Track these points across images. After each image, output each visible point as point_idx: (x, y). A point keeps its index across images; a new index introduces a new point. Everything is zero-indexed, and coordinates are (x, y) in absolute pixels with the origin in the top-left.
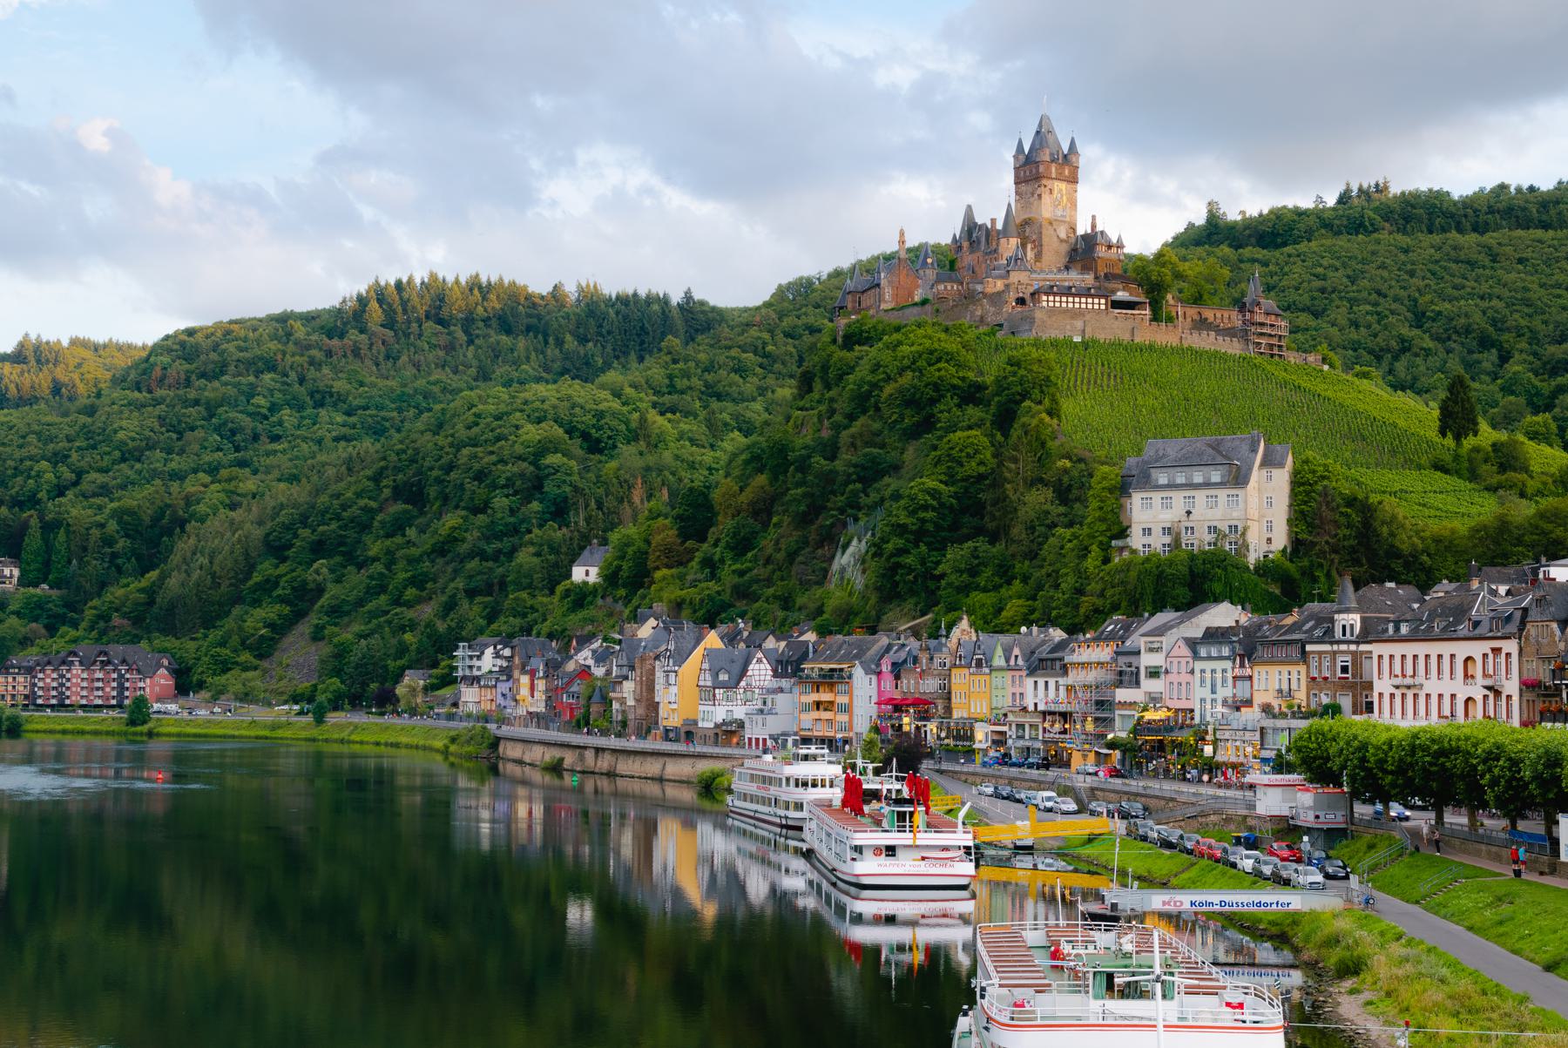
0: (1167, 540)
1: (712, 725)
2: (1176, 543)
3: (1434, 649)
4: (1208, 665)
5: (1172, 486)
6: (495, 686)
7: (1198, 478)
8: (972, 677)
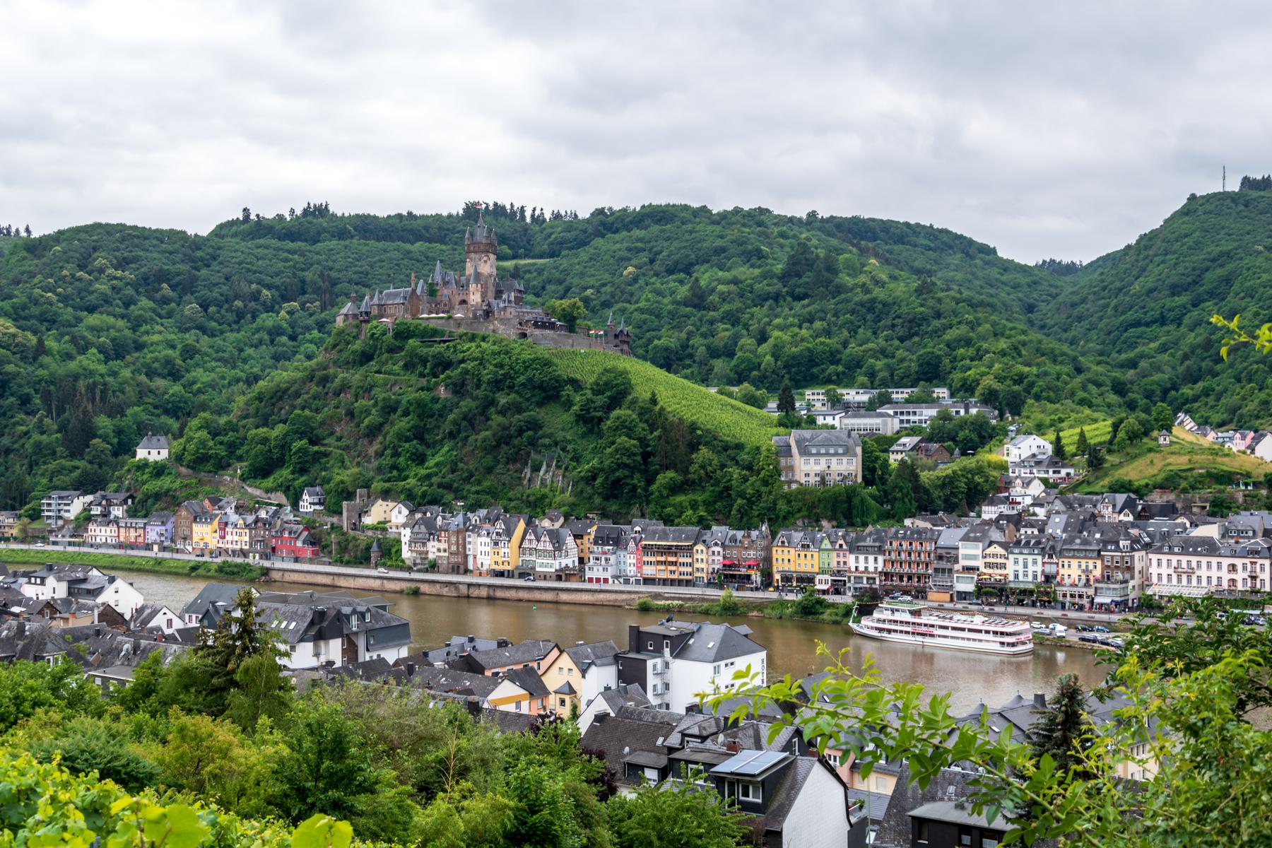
0: (818, 479)
2: (823, 482)
3: (1204, 560)
4: (1021, 558)
5: (818, 454)
6: (144, 528)
7: (823, 451)
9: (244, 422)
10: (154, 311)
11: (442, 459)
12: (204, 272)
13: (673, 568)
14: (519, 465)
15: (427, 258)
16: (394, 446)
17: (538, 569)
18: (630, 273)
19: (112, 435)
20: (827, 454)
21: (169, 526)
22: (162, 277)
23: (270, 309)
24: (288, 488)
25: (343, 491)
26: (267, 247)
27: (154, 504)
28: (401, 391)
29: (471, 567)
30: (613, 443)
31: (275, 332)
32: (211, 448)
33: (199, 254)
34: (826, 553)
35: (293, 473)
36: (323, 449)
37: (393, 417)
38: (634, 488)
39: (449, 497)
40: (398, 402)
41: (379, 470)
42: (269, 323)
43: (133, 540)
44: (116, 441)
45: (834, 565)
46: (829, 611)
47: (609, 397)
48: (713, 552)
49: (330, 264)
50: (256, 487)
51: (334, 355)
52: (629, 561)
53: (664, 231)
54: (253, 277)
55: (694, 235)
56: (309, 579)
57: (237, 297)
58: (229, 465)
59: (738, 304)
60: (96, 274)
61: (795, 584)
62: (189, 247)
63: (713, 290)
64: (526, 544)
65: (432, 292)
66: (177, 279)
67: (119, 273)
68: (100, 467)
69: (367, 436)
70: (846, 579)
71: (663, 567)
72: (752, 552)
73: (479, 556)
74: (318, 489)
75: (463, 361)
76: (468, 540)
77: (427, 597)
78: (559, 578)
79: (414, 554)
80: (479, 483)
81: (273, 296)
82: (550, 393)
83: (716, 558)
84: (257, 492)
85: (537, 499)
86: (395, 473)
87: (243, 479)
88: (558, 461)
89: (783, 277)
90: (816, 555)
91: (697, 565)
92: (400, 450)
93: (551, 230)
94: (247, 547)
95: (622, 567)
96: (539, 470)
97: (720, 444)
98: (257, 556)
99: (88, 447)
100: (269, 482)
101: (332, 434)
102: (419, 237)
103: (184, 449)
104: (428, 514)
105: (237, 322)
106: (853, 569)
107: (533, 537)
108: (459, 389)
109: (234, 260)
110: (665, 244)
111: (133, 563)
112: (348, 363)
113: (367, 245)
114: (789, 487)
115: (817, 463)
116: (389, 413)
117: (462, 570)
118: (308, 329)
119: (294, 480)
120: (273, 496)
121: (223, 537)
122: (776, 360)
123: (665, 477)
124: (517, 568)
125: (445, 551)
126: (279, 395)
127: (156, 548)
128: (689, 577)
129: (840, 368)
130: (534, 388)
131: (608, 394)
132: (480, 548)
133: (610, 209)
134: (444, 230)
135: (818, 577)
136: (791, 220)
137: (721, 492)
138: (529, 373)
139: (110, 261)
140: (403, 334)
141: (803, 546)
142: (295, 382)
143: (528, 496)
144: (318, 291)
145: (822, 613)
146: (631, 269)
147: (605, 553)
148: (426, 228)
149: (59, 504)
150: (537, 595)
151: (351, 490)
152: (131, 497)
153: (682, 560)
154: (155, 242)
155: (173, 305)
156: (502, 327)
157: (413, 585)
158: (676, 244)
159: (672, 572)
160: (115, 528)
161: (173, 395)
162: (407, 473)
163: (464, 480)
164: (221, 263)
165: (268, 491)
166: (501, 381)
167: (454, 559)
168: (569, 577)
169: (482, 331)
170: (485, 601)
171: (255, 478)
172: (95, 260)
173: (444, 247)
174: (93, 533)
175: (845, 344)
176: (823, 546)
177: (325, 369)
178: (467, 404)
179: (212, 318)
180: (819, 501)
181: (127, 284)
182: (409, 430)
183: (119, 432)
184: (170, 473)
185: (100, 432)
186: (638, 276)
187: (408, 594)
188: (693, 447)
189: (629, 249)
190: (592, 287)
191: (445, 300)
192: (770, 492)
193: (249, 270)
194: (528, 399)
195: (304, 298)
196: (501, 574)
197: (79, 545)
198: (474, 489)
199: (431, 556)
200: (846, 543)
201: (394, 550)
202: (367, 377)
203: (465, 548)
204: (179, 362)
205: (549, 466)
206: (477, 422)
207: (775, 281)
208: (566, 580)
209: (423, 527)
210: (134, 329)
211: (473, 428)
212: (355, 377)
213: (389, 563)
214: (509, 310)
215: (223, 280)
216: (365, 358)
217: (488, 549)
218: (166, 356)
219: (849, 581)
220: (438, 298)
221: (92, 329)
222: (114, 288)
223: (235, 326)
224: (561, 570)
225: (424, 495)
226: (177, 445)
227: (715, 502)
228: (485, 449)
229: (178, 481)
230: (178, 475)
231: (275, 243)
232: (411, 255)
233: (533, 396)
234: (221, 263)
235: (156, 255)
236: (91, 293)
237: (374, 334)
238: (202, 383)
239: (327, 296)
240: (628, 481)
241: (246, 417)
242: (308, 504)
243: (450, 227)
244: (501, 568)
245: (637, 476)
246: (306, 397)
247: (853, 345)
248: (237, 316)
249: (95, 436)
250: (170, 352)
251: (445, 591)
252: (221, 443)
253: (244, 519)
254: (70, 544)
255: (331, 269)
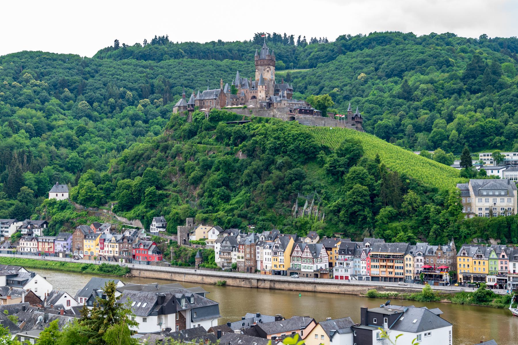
1: (313, 271)
2: (491, 213)
5: (488, 195)
6: (54, 243)
7: (491, 193)
8: (474, 261)
9: (115, 175)
10: (59, 106)
11: (240, 198)
12: (91, 80)
13: (391, 270)
14: (290, 203)
15: (231, 69)
16: (210, 191)
17: (302, 270)
18: (362, 78)
19: (34, 184)
20: (494, 195)
21: (69, 241)
22: (64, 84)
23: (132, 103)
24: (143, 217)
25: (177, 219)
26: (129, 65)
27: (60, 227)
28: (214, 155)
29: (259, 268)
30: (351, 188)
31: (135, 118)
32: (95, 192)
33: (87, 69)
34: (493, 261)
35: (146, 207)
36: (165, 192)
37: (209, 172)
38: (365, 217)
39: (245, 223)
40: (212, 162)
41: (201, 206)
42: (131, 112)
43: (47, 250)
44: (36, 187)
45: (499, 269)
46: (495, 300)
47: (348, 158)
48: (418, 260)
49: (169, 74)
50: (123, 217)
51: (171, 132)
52: (362, 265)
53: (383, 49)
54: (119, 83)
55: (404, 52)
56: (156, 275)
57: (111, 96)
58: (106, 203)
59: (433, 97)
60: (24, 83)
61: (472, 281)
62: (81, 65)
63: (417, 88)
64: (295, 254)
65: (234, 91)
66: (74, 85)
67: (38, 82)
68: (27, 204)
69: (193, 184)
70: (507, 278)
71: (384, 269)
72: (443, 260)
73: (264, 262)
74: (162, 218)
75: (253, 135)
76: (257, 251)
77: (231, 288)
78: (316, 276)
79: (223, 260)
80: (264, 214)
81: (133, 95)
82: (310, 156)
83: (419, 264)
84: (124, 220)
85: (302, 224)
86: (211, 208)
87: (115, 211)
88: (315, 200)
89: (463, 79)
90: (486, 262)
91: (406, 268)
92: (214, 193)
93: (311, 50)
94: (118, 255)
95: (357, 269)
96: (303, 206)
97: (422, 188)
98: (124, 260)
99: (19, 191)
100: (131, 214)
101: (171, 182)
102: (225, 56)
103: (78, 193)
104: (232, 234)
105: (111, 112)
106: (512, 272)
107: (299, 249)
108: (251, 153)
109: (108, 73)
110: (385, 58)
111: (47, 264)
112: (180, 137)
113: (193, 62)
114: (468, 217)
115: (487, 201)
116: (207, 169)
117: (253, 270)
118: (155, 116)
119: (147, 212)
120: (133, 222)
121: (102, 249)
122: (459, 133)
123: (386, 210)
124: (289, 269)
125: (242, 258)
126: (137, 158)
127: (61, 255)
128: (401, 276)
129: (503, 138)
130: (300, 152)
131: (348, 156)
132: (265, 256)
133: (349, 36)
134: (242, 51)
135: (488, 277)
136: (469, 41)
137: (423, 220)
138: (297, 143)
139: (33, 75)
140: (215, 118)
141: (478, 256)
142: (147, 150)
143: (296, 223)
144: (162, 91)
145: (491, 301)
146: (363, 75)
147: (346, 260)
148: (230, 50)
149: (2, 228)
150: (302, 287)
151: (182, 218)
152: (46, 223)
153: (396, 265)
154: (60, 62)
155: (71, 102)
156: (279, 113)
157: (222, 280)
158: (392, 58)
159: (391, 273)
160: (36, 242)
161: (72, 158)
162: (218, 208)
163: (255, 212)
164: (101, 75)
165: (130, 219)
166: (278, 148)
167: (248, 264)
168: (322, 275)
169: (266, 116)
170: (268, 290)
171: (122, 211)
172: (23, 74)
173: (241, 62)
174: (22, 246)
175: (506, 122)
176: (491, 257)
177: (166, 141)
178: (256, 163)
179: (96, 110)
180: (488, 226)
181: (43, 89)
182: (219, 180)
183: (38, 182)
184: (70, 208)
185: (26, 182)
186: (367, 79)
187: (219, 285)
188: (404, 191)
189: (361, 62)
190: (338, 87)
191: (242, 96)
192: (456, 221)
193: (118, 79)
194: (295, 160)
195: (153, 96)
196: (278, 273)
197: (14, 253)
198: (261, 218)
199: (234, 261)
200: (507, 254)
201: (210, 257)
202: (192, 146)
203: (255, 256)
204: (75, 137)
205: (309, 203)
206: (263, 175)
207: (458, 81)
208: (321, 278)
209: (228, 242)
210: (48, 117)
211: (261, 179)
212: (185, 146)
213: (207, 266)
214: (283, 102)
215: (102, 86)
216: (191, 134)
217: (270, 257)
218: (67, 134)
219: (509, 280)
220: (238, 95)
221: (22, 117)
222: (35, 92)
223: (110, 115)
224: (318, 271)
225: (229, 222)
226: (74, 190)
227: (419, 227)
228: (268, 192)
229: (75, 213)
230: (75, 209)
231: (134, 61)
232: (220, 68)
233: (299, 157)
234: (101, 75)
235: (61, 70)
236: (21, 95)
237: (197, 119)
238: (90, 151)
239: (168, 95)
240: (361, 213)
241: (117, 172)
242: (155, 227)
243: (246, 49)
244: (278, 269)
245: (367, 209)
246: (154, 159)
247: (511, 123)
248: (111, 108)
249: (24, 185)
250: (69, 131)
251: (243, 284)
252: (101, 189)
253: (115, 237)
254: (8, 252)
255: (170, 77)
